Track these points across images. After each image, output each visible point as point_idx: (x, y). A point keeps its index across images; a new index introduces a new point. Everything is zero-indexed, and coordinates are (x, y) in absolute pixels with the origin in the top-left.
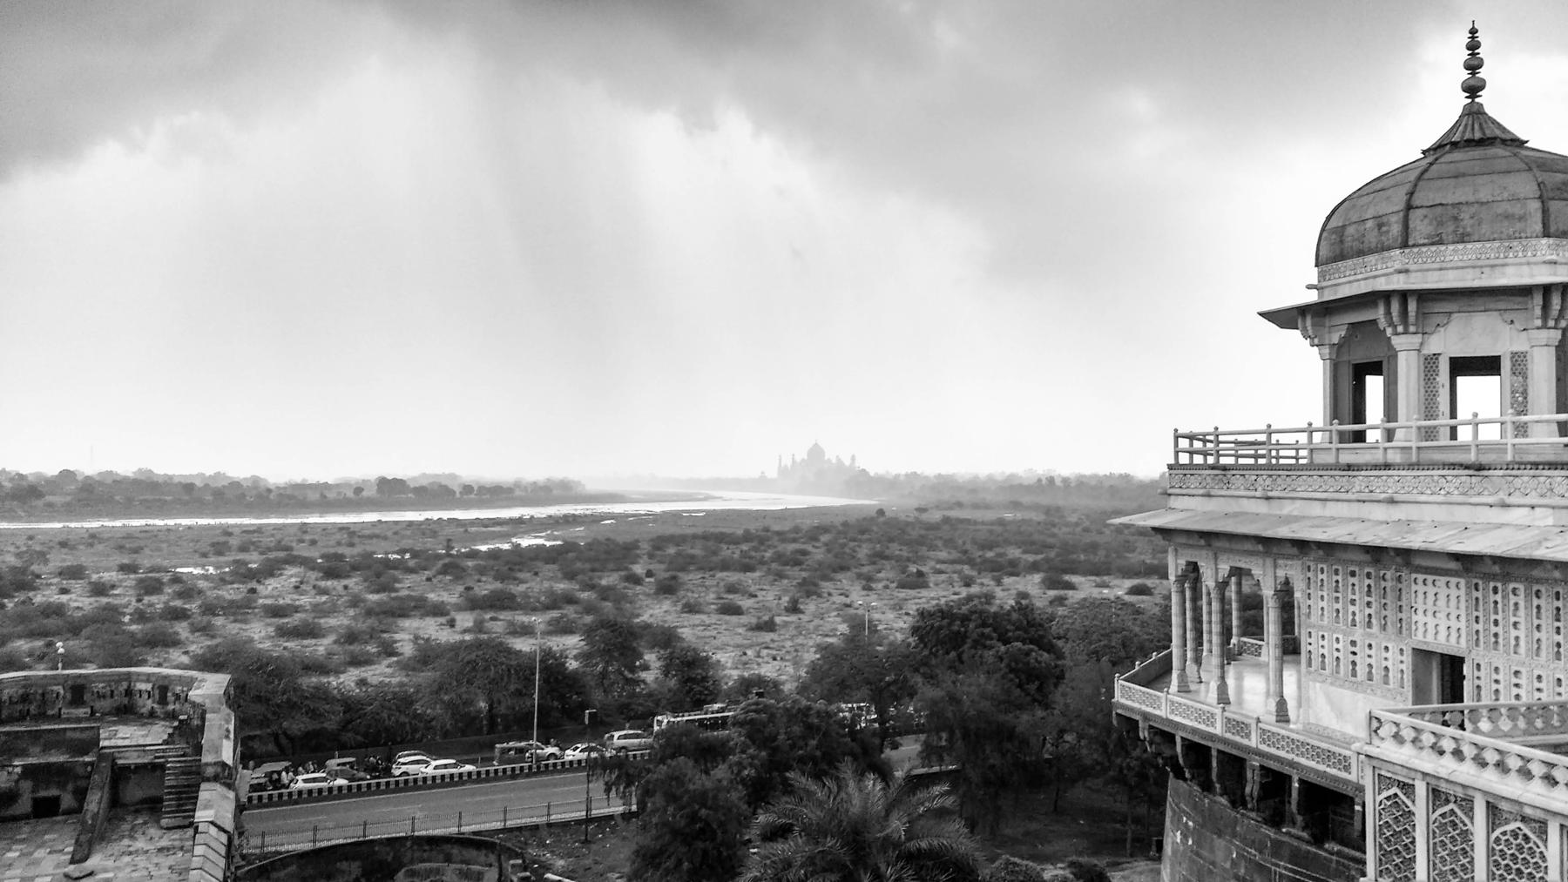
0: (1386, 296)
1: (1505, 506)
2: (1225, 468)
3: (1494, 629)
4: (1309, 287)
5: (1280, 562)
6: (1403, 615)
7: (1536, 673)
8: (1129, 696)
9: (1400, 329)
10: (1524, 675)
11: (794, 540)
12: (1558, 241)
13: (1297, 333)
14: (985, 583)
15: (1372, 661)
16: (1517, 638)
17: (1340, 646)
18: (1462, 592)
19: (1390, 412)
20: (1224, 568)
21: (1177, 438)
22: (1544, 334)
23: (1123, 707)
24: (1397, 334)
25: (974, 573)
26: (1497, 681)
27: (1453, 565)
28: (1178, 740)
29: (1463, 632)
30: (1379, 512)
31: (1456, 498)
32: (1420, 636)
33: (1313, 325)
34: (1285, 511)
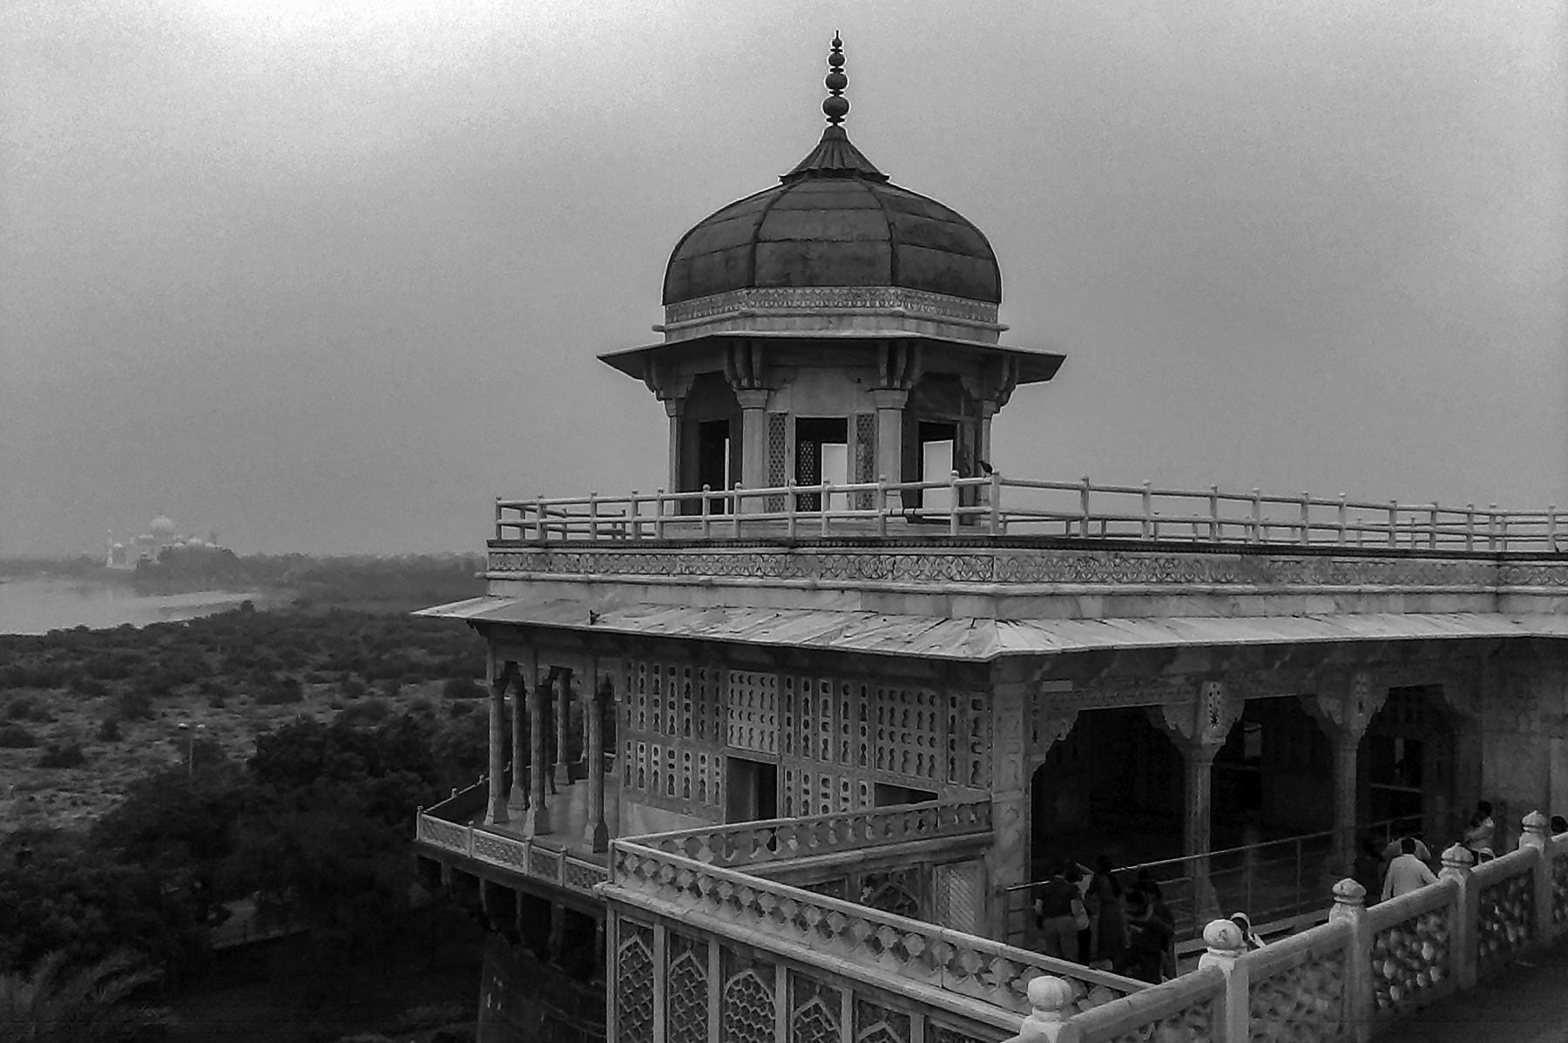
1: (816, 589)
4: (658, 329)
8: (434, 832)
9: (745, 383)
11: (121, 644)
14: (376, 693)
15: (689, 774)
16: (825, 742)
18: (775, 691)
20: (545, 668)
23: (424, 846)
25: (363, 682)
27: (767, 659)
28: (482, 884)
32: (735, 744)
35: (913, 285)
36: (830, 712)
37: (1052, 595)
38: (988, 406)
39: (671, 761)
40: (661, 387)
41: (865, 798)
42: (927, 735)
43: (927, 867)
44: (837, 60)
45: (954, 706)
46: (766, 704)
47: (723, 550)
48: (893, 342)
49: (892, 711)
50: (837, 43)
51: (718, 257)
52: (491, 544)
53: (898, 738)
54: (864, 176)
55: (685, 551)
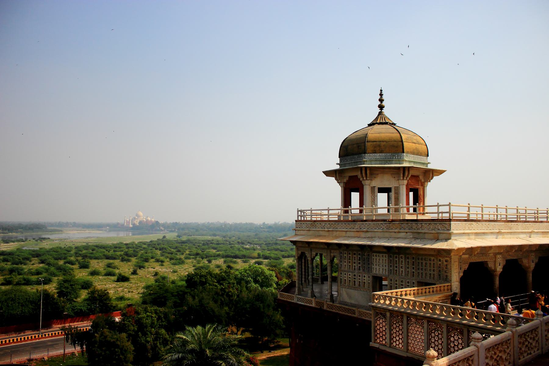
1: (399, 232)
3: (395, 269)
4: (337, 164)
9: (365, 178)
15: (360, 281)
18: (387, 258)
19: (361, 203)
20: (314, 253)
21: (298, 211)
24: (363, 180)
26: (396, 284)
27: (385, 250)
30: (363, 235)
31: (385, 230)
32: (374, 271)
33: (339, 176)
35: (408, 153)
36: (403, 263)
44: (381, 95)
45: (440, 261)
46: (384, 261)
48: (404, 168)
49: (422, 263)
50: (381, 90)
51: (355, 145)
52: (296, 221)
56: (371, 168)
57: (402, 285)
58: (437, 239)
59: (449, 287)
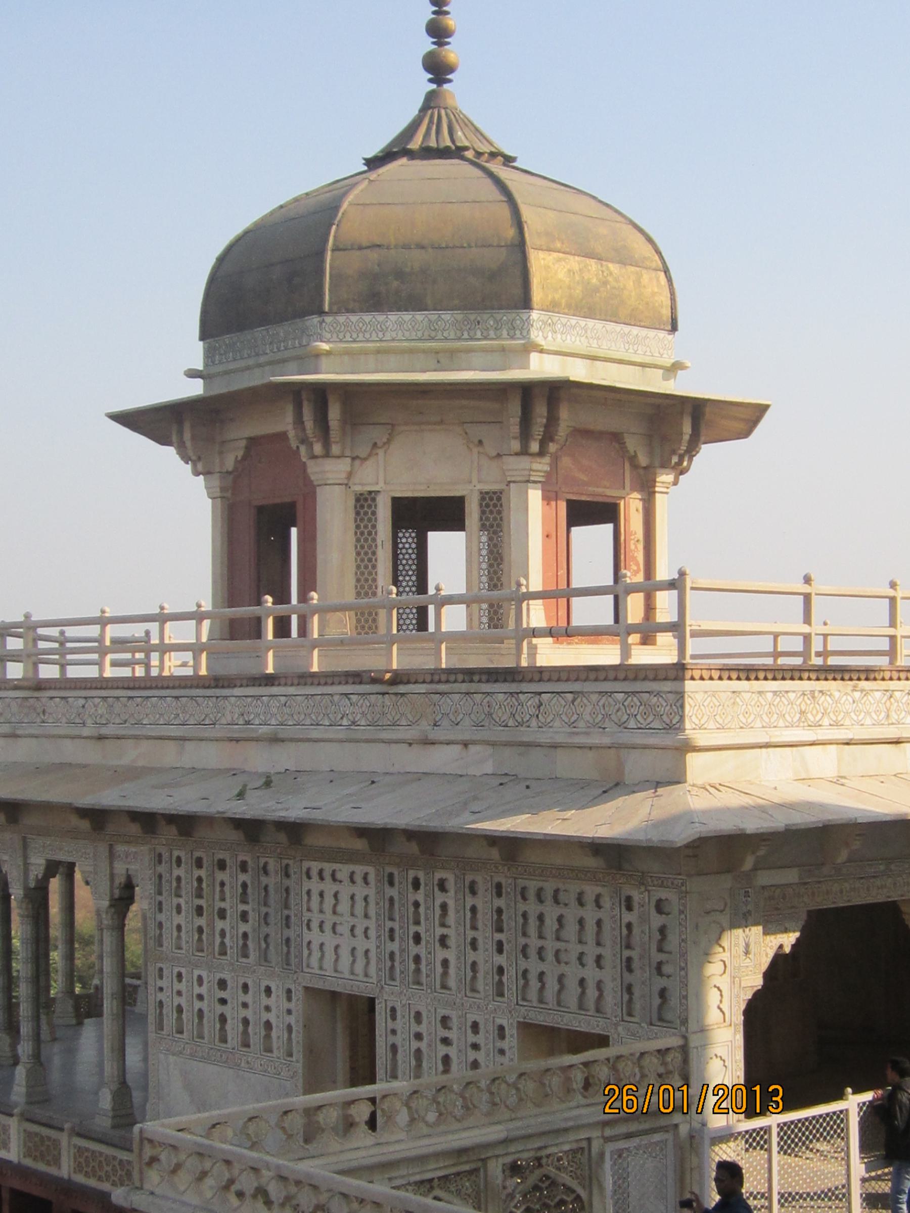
0: (296, 392)
1: (427, 742)
2: (41, 686)
4: (192, 374)
5: (120, 849)
6: (291, 933)
7: (471, 1018)
9: (318, 449)
10: (455, 1023)
12: (544, 316)
13: (170, 452)
15: (249, 1013)
16: (445, 963)
17: (203, 990)
18: (371, 891)
20: (38, 864)
22: (524, 462)
24: (314, 457)
26: (419, 1036)
27: (360, 844)
29: (373, 955)
33: (193, 438)
34: (126, 761)
35: (552, 307)
37: (767, 746)
38: (664, 478)
39: (223, 994)
40: (198, 458)
41: (505, 1045)
42: (591, 951)
43: (596, 1146)
45: (629, 908)
47: (291, 690)
49: (541, 918)
53: (550, 956)
54: (479, 154)
55: (237, 691)
56: (350, 393)
57: (446, 1041)
58: (613, 785)
59: (674, 1059)
